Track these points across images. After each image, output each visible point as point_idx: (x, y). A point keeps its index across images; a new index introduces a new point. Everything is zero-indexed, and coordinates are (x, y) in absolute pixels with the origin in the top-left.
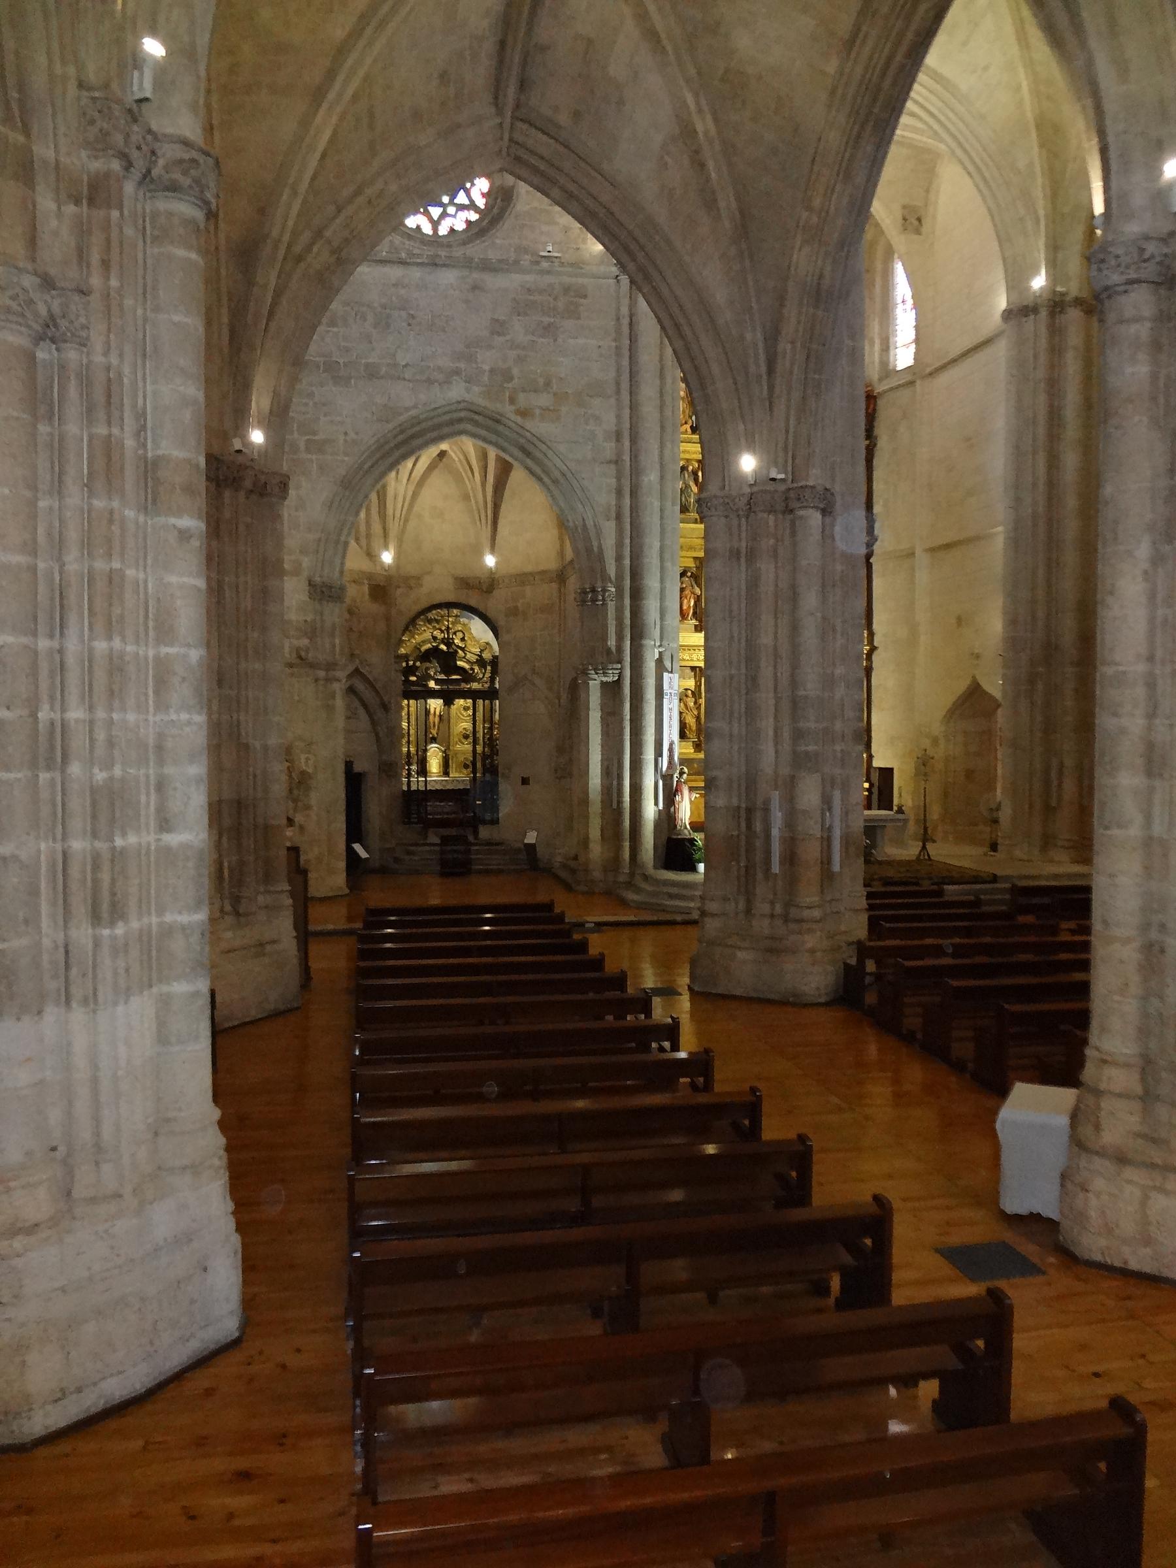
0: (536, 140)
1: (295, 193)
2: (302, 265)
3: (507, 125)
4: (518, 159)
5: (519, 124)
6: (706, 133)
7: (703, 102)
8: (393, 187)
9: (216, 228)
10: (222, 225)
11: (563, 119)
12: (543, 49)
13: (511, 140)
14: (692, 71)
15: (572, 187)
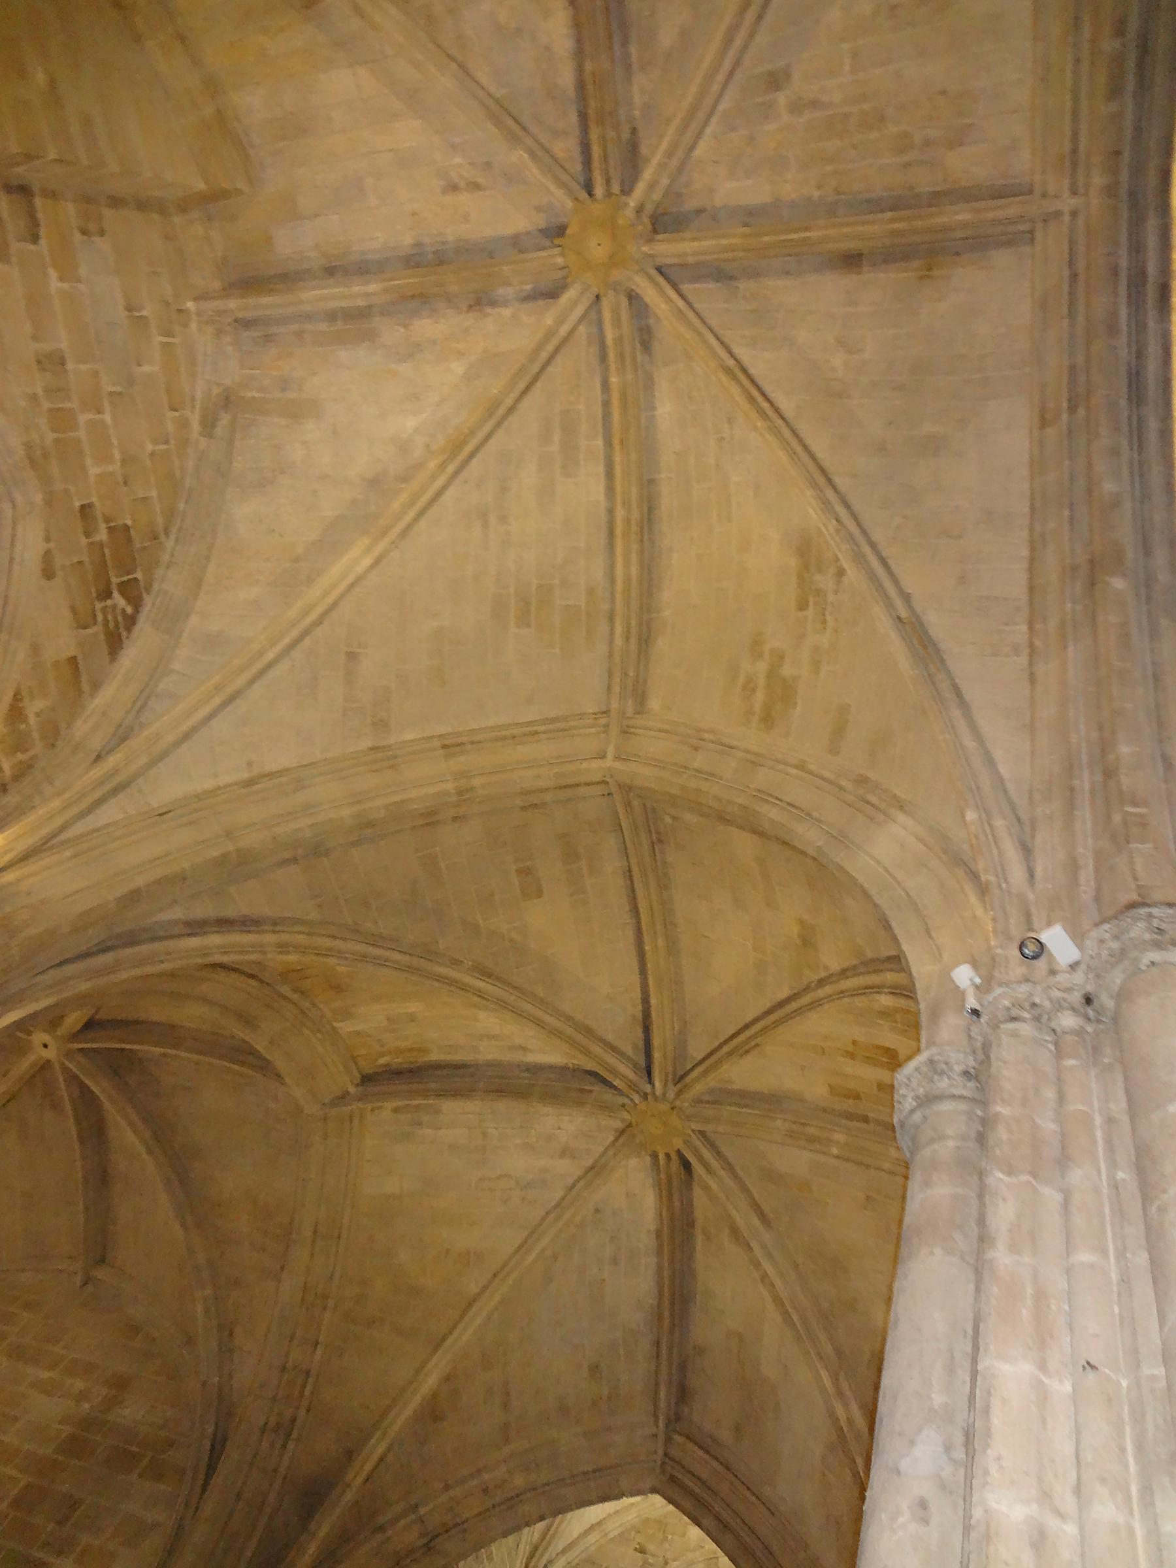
0: (693, 1456)
1: (384, 1434)
2: (379, 1537)
3: (661, 1436)
4: (673, 1479)
5: (677, 1438)
6: (850, 1421)
7: (845, 1385)
8: (519, 1481)
9: (284, 1446)
10: (291, 1446)
11: (725, 1435)
12: (700, 1351)
13: (666, 1455)
14: (829, 1349)
15: (726, 1515)
